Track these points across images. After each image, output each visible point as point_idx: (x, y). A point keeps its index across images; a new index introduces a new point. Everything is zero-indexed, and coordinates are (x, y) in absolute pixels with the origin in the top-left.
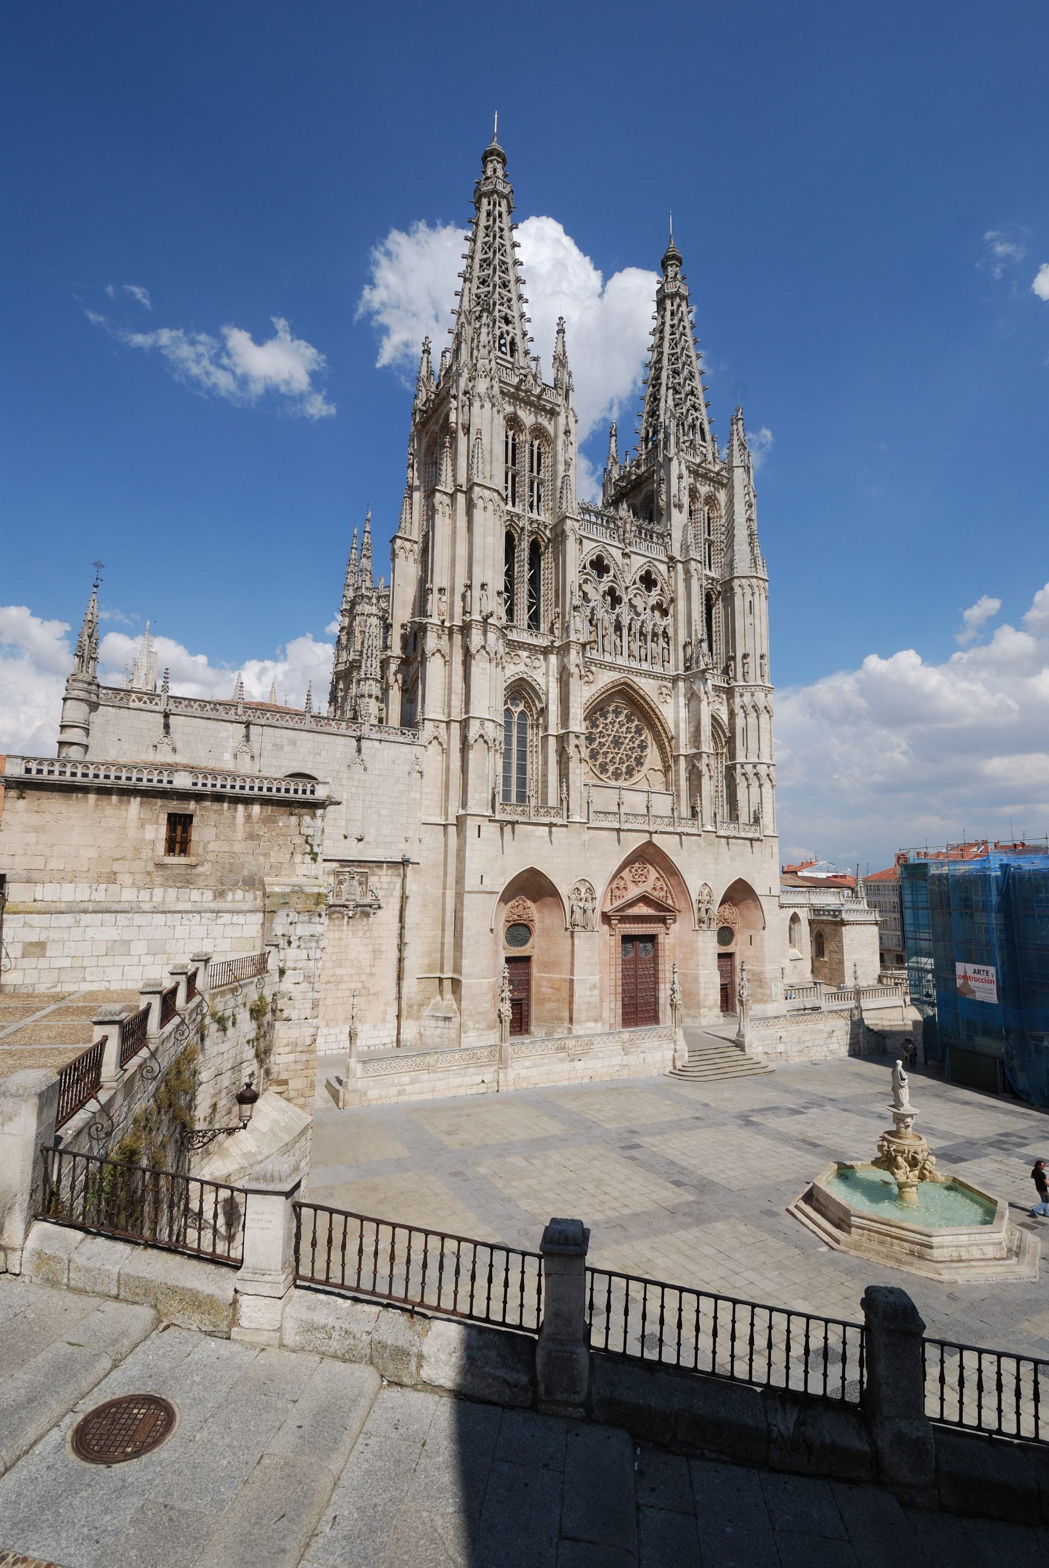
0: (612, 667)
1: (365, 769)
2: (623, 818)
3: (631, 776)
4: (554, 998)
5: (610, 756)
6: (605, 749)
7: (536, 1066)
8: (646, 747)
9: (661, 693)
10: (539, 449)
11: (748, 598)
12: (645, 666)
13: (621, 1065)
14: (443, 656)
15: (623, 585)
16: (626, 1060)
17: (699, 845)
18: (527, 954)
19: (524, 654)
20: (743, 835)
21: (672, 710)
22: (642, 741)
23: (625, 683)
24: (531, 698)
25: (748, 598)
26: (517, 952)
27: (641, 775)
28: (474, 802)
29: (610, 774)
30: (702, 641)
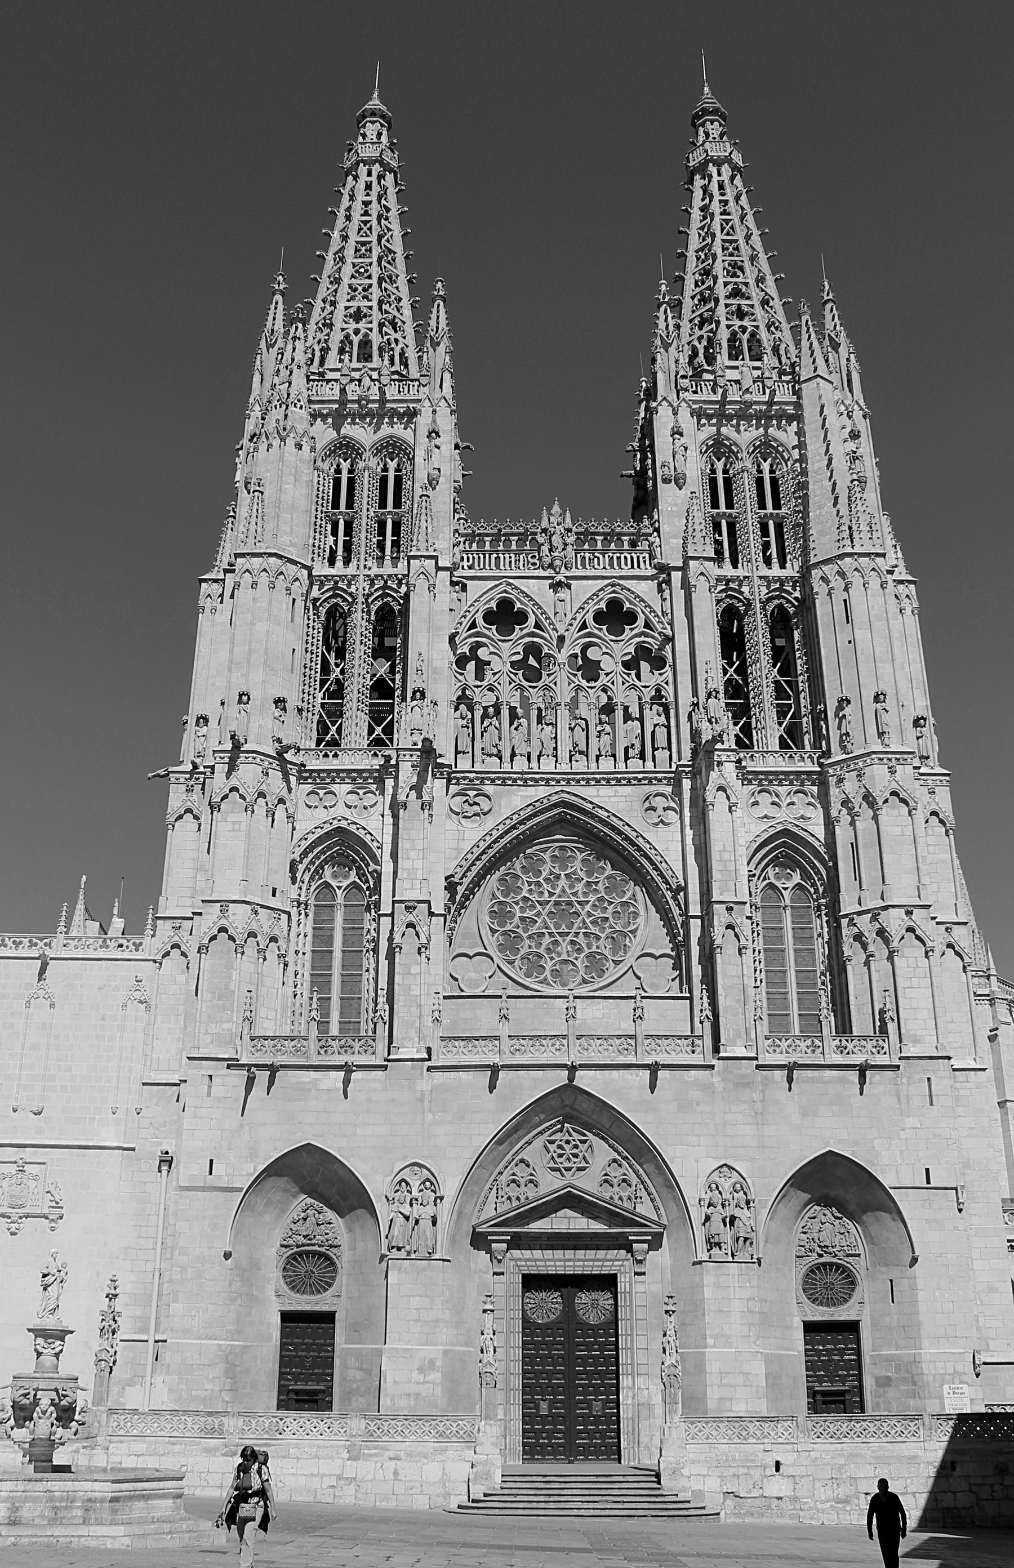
1: (52, 1006)
2: (506, 1043)
3: (601, 973)
4: (363, 1389)
5: (547, 940)
6: (534, 930)
7: (155, 1454)
8: (636, 914)
9: (654, 809)
11: (839, 595)
13: (339, 1477)
15: (555, 635)
16: (352, 1469)
17: (708, 1088)
18: (325, 1308)
19: (342, 789)
20: (838, 1059)
23: (564, 804)
24: (363, 859)
25: (839, 595)
27: (623, 968)
28: (209, 1038)
29: (547, 973)
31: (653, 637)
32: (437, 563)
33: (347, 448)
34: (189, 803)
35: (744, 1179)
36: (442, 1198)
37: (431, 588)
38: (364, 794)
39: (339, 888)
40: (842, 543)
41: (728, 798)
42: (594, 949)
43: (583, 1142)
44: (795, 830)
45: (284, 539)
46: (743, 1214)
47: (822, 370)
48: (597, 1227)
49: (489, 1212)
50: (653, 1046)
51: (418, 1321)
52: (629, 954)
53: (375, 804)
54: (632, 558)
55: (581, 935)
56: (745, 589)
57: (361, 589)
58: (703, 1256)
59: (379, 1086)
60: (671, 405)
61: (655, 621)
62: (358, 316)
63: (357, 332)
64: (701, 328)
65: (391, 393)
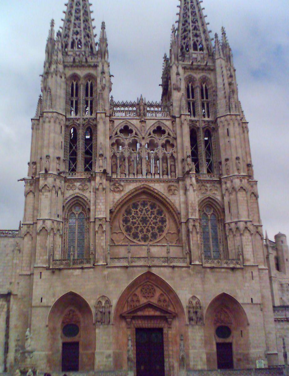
0: (136, 181)
2: (130, 259)
3: (155, 238)
5: (140, 229)
6: (136, 225)
8: (165, 221)
10: (91, 84)
12: (157, 177)
14: (34, 193)
17: (189, 274)
21: (178, 198)
22: (162, 218)
23: (144, 188)
26: (69, 340)
27: (162, 237)
28: (40, 261)
29: (140, 238)
30: (188, 157)
31: (170, 138)
32: (105, 114)
33: (75, 77)
34: (31, 189)
35: (199, 300)
36: (112, 306)
37: (104, 123)
38: (84, 185)
39: (77, 214)
40: (227, 111)
41: (193, 187)
42: (154, 231)
43: (152, 288)
44: (212, 197)
45: (58, 107)
46: (199, 310)
47: (222, 56)
48: (158, 313)
49: (125, 310)
50: (173, 260)
51: (105, 343)
52: (164, 233)
53: (88, 189)
54: (164, 113)
55: (150, 227)
56: (197, 124)
57: (81, 122)
58: (188, 323)
59: (91, 273)
60: (176, 65)
61: (171, 133)
62: (77, 33)
63: (77, 39)
64: (185, 40)
65: (89, 59)
